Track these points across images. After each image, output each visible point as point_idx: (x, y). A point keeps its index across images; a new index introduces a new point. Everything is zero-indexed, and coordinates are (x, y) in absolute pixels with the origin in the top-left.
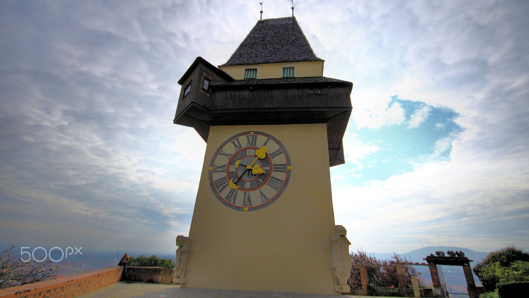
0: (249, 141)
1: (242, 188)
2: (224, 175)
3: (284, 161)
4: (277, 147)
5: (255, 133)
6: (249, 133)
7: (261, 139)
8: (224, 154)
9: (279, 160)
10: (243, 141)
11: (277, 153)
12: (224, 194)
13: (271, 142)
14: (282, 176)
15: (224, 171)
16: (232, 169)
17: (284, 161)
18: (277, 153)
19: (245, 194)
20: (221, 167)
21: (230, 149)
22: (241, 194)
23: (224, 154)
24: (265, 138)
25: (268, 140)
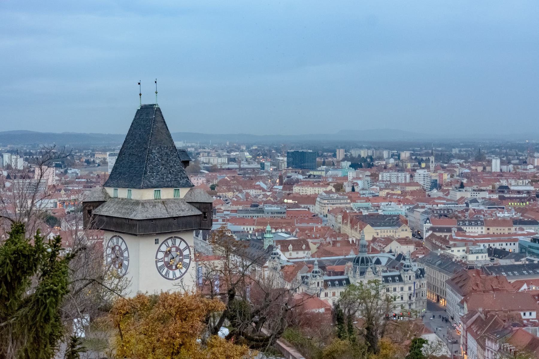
1: (172, 269)
2: (163, 263)
3: (188, 253)
4: (185, 245)
5: (175, 237)
6: (172, 238)
7: (178, 241)
9: (186, 252)
10: (170, 242)
11: (185, 249)
12: (164, 273)
13: (182, 242)
16: (166, 259)
17: (188, 253)
18: (185, 249)
21: (164, 248)
22: (171, 272)
24: (180, 240)
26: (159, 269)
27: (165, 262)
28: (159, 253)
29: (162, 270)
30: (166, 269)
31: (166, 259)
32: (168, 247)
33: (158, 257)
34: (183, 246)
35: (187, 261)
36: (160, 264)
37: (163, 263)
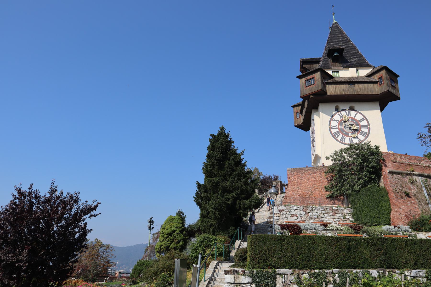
0: (347, 114)
2: (337, 130)
8: (335, 120)
9: (364, 123)
11: (362, 120)
12: (339, 138)
13: (358, 114)
14: (366, 130)
15: (337, 128)
16: (341, 127)
18: (362, 120)
19: (350, 139)
20: (335, 126)
23: (335, 120)
25: (356, 114)
26: (334, 135)
27: (340, 130)
28: (332, 122)
29: (337, 136)
30: (341, 135)
31: (341, 127)
32: (341, 116)
33: (331, 124)
34: (359, 117)
35: (366, 130)
36: (334, 131)
37: (337, 130)
